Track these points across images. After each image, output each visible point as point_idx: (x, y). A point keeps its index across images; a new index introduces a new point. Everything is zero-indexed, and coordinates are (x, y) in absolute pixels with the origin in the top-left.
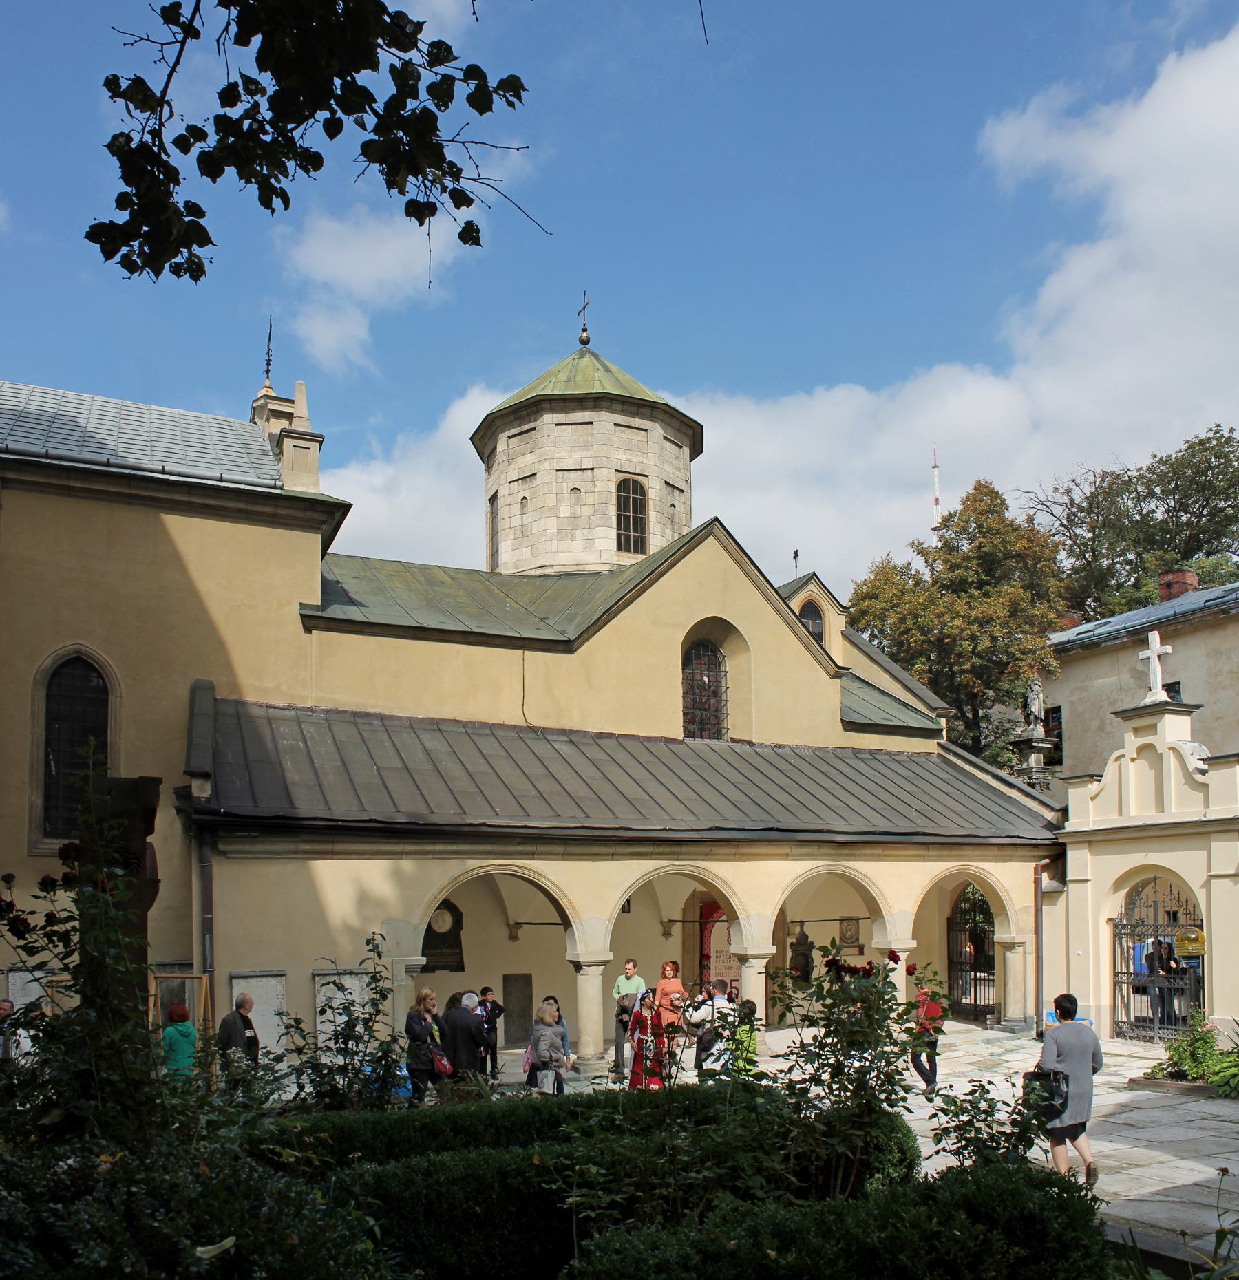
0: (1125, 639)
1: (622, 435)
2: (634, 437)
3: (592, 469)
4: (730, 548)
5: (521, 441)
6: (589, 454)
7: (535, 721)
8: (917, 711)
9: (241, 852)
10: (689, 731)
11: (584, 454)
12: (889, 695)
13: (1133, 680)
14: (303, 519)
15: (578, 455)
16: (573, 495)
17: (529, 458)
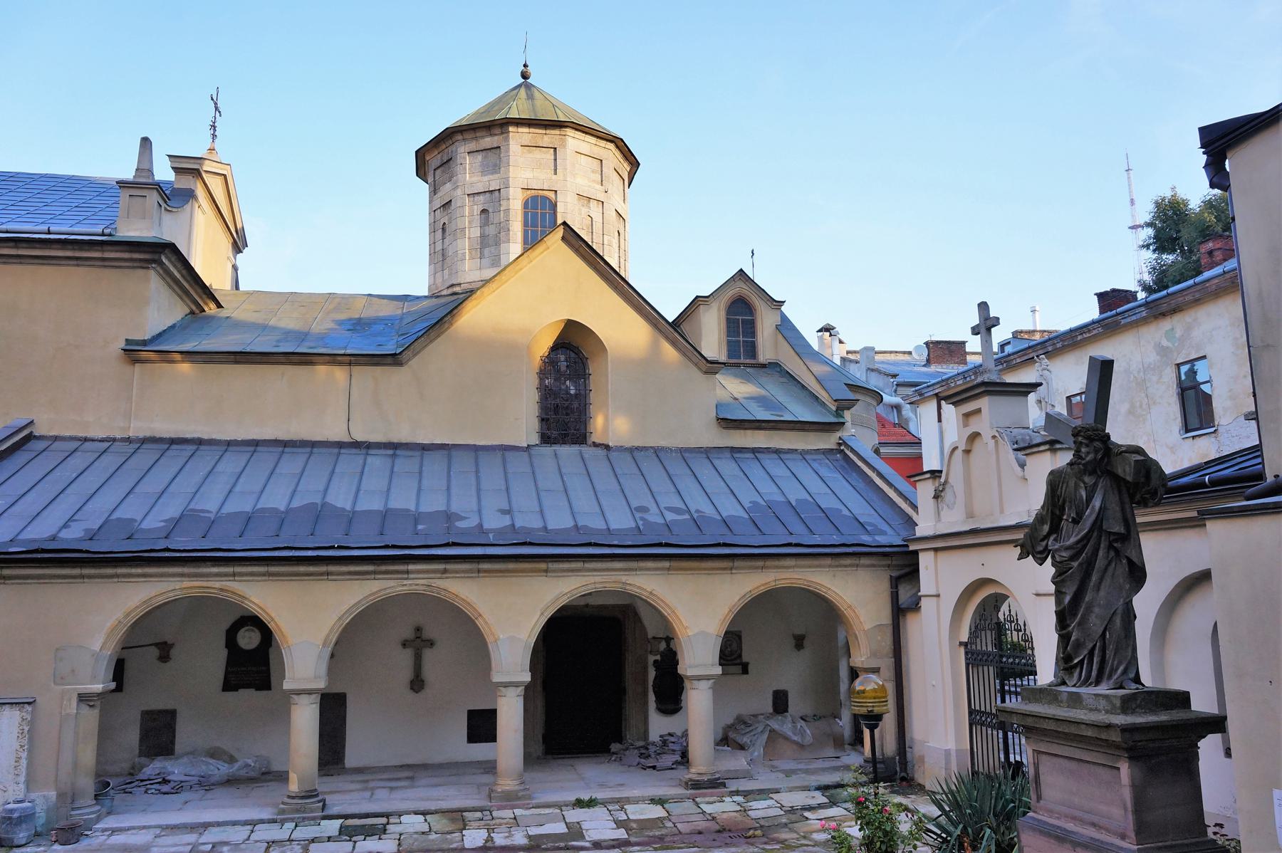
0: (1144, 314)
1: (531, 155)
2: (543, 156)
3: (500, 189)
4: (581, 249)
5: (443, 172)
6: (496, 176)
7: (359, 437)
8: (823, 404)
9: (125, 576)
10: (549, 438)
11: (491, 177)
12: (807, 389)
13: (1158, 357)
14: (131, 260)
15: (486, 178)
16: (483, 216)
17: (448, 186)
